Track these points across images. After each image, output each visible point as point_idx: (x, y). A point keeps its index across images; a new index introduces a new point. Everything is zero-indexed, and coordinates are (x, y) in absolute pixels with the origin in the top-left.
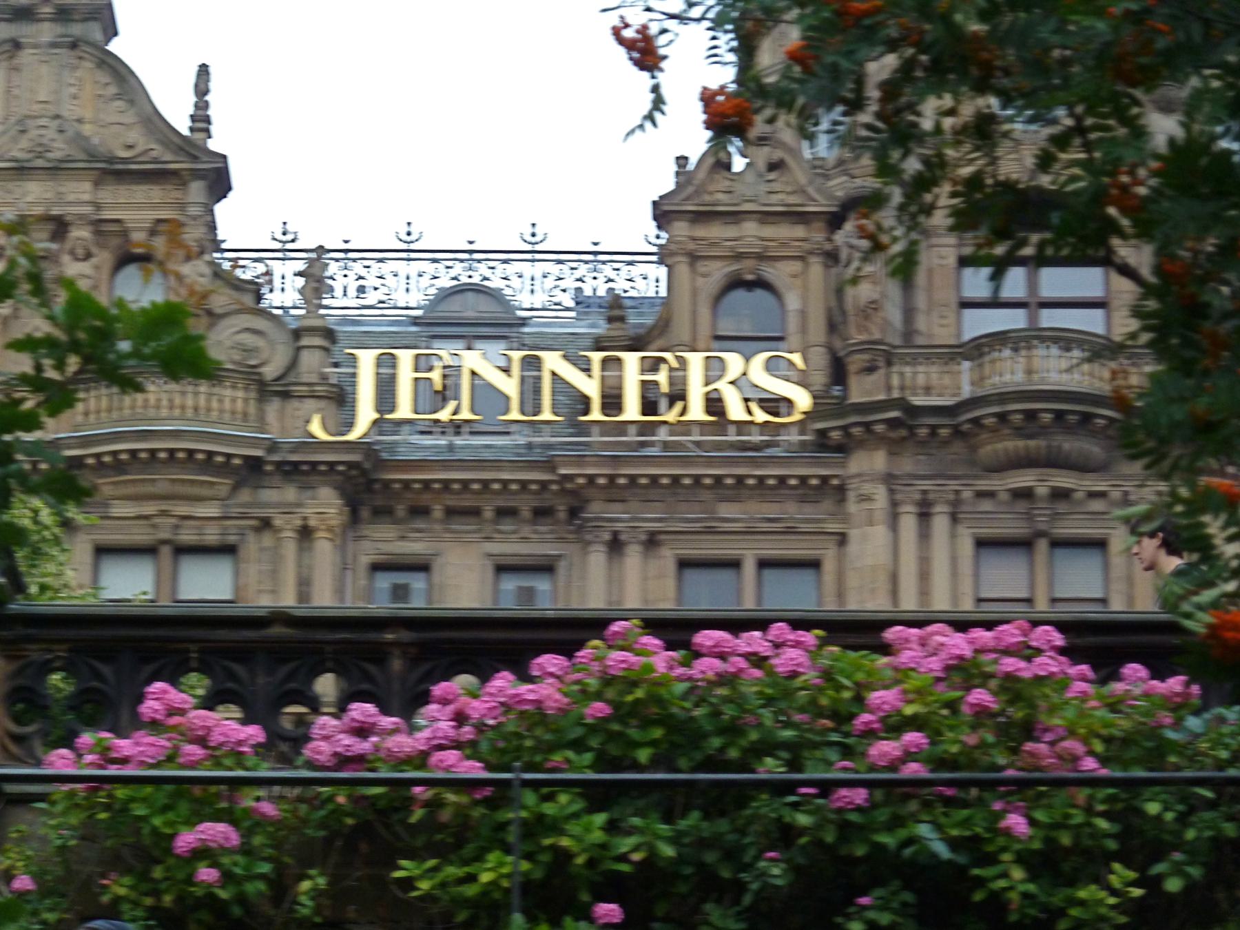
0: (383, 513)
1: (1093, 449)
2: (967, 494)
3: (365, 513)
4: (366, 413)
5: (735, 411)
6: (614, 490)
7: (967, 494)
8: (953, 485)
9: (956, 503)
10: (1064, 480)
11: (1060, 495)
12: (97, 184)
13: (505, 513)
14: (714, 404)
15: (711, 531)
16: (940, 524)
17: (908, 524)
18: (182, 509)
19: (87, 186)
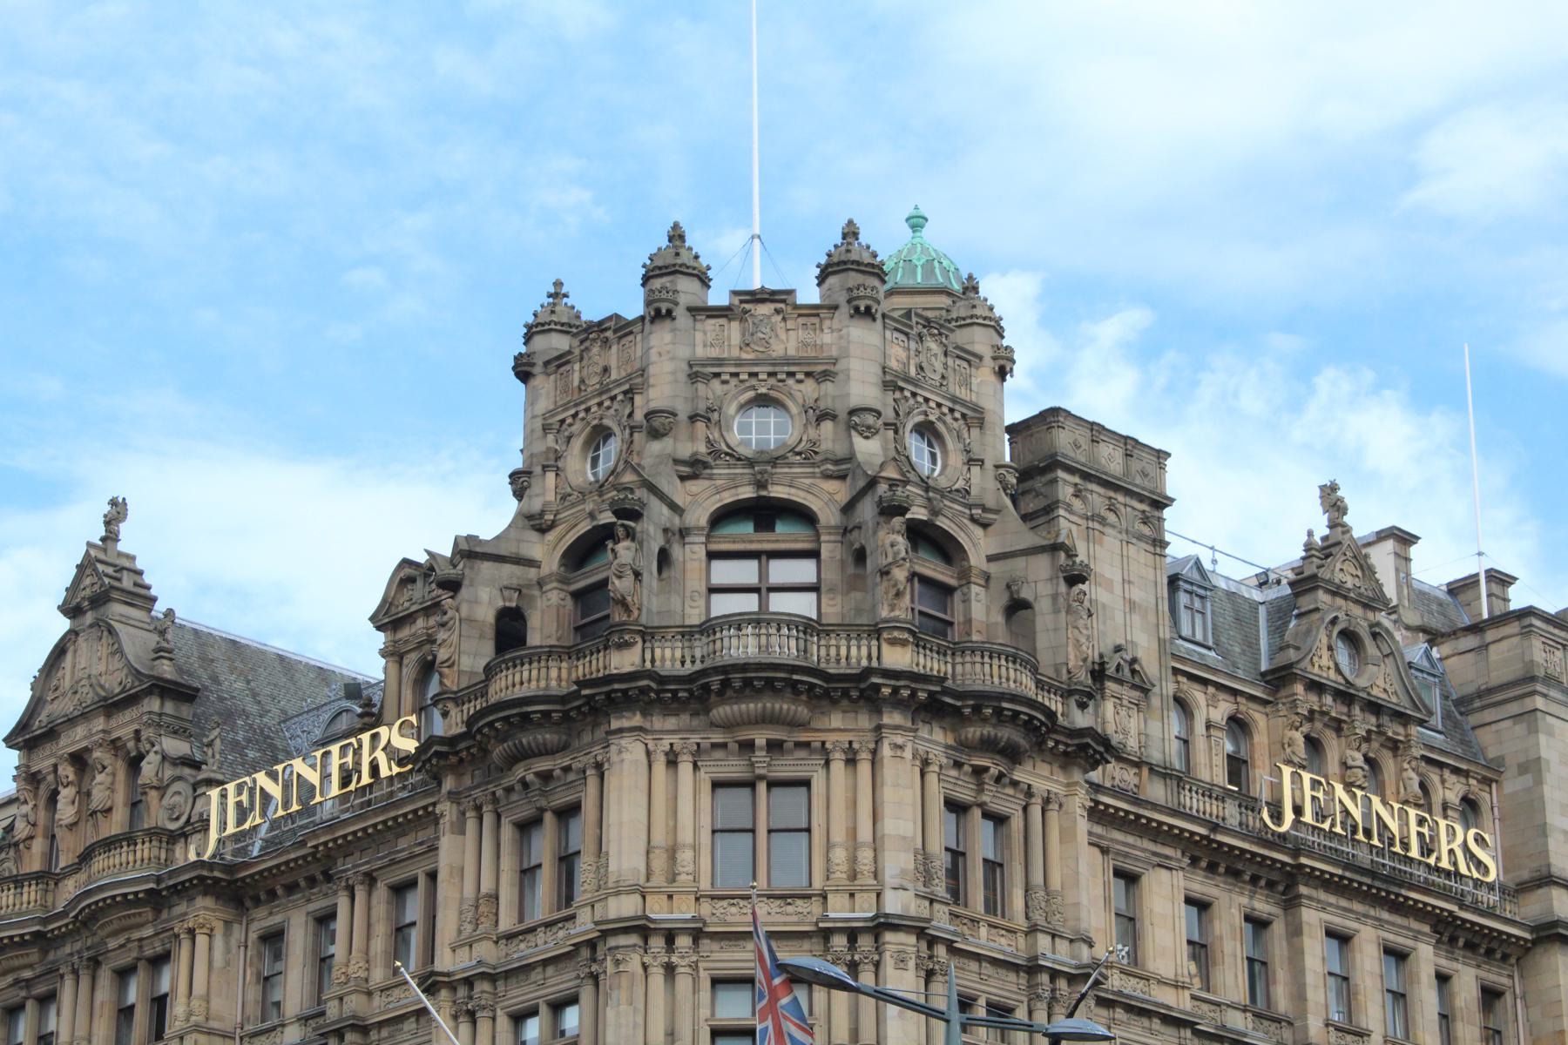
0: (257, 902)
1: (549, 737)
2: (499, 793)
3: (248, 903)
4: (213, 835)
5: (384, 772)
6: (348, 847)
7: (499, 793)
8: (491, 788)
9: (495, 800)
10: (543, 765)
11: (546, 777)
12: (108, 716)
13: (312, 881)
14: (374, 769)
15: (393, 863)
16: (488, 819)
17: (471, 825)
18: (136, 935)
19: (102, 719)
